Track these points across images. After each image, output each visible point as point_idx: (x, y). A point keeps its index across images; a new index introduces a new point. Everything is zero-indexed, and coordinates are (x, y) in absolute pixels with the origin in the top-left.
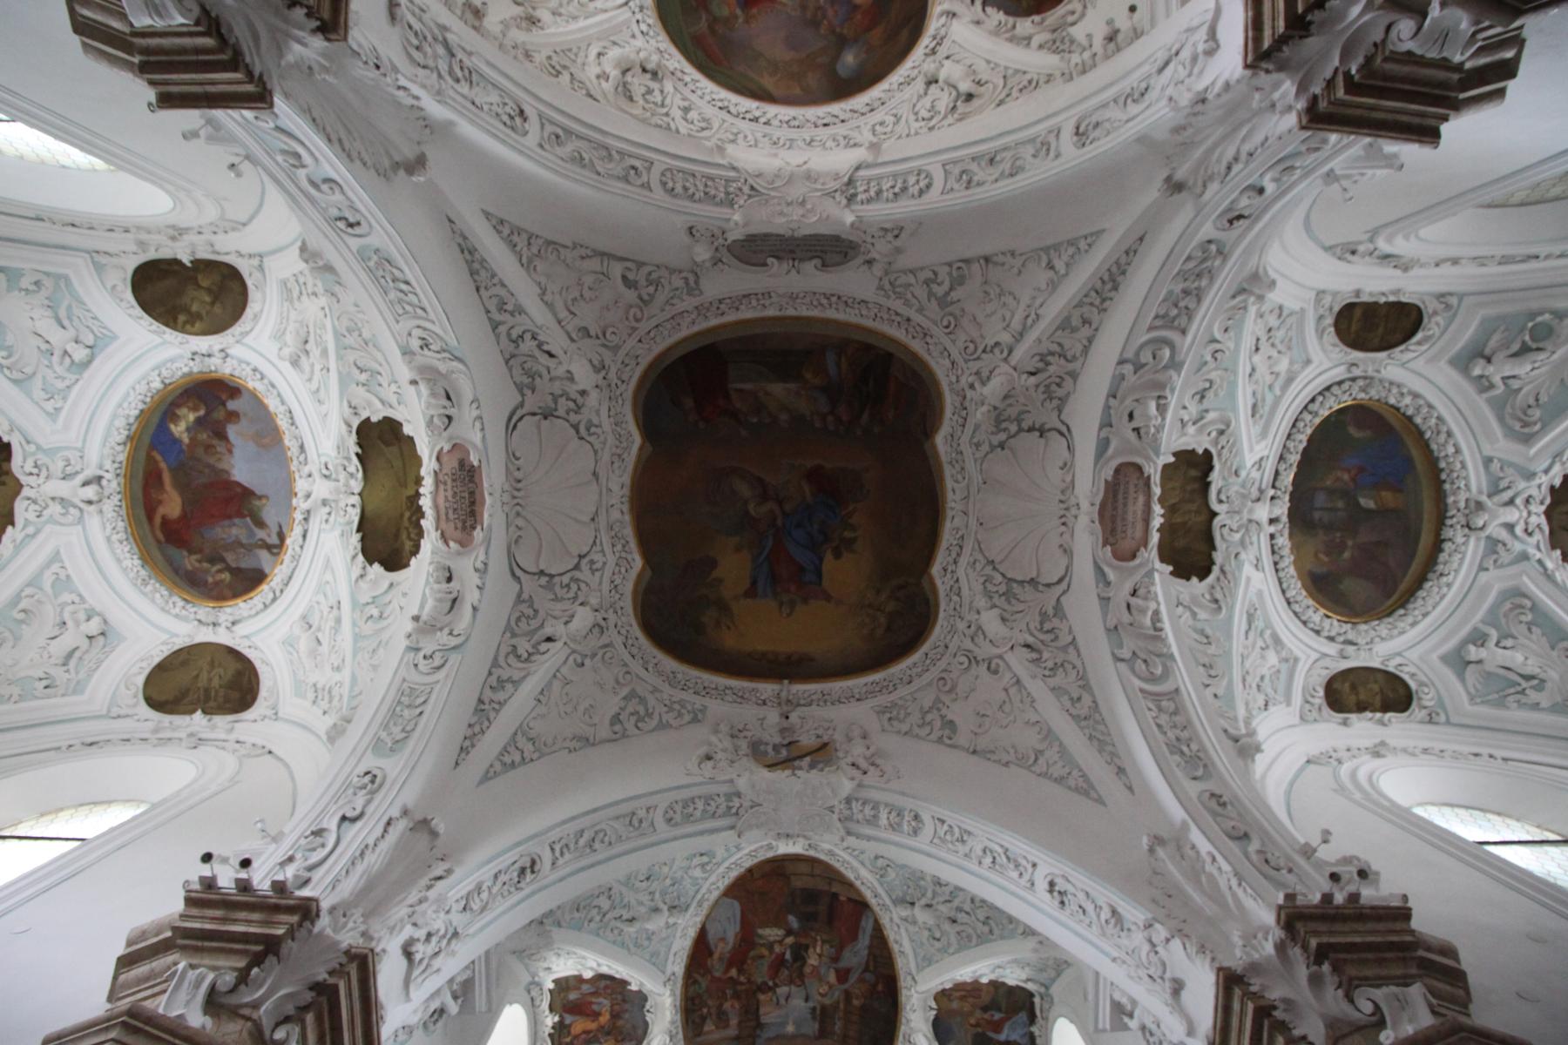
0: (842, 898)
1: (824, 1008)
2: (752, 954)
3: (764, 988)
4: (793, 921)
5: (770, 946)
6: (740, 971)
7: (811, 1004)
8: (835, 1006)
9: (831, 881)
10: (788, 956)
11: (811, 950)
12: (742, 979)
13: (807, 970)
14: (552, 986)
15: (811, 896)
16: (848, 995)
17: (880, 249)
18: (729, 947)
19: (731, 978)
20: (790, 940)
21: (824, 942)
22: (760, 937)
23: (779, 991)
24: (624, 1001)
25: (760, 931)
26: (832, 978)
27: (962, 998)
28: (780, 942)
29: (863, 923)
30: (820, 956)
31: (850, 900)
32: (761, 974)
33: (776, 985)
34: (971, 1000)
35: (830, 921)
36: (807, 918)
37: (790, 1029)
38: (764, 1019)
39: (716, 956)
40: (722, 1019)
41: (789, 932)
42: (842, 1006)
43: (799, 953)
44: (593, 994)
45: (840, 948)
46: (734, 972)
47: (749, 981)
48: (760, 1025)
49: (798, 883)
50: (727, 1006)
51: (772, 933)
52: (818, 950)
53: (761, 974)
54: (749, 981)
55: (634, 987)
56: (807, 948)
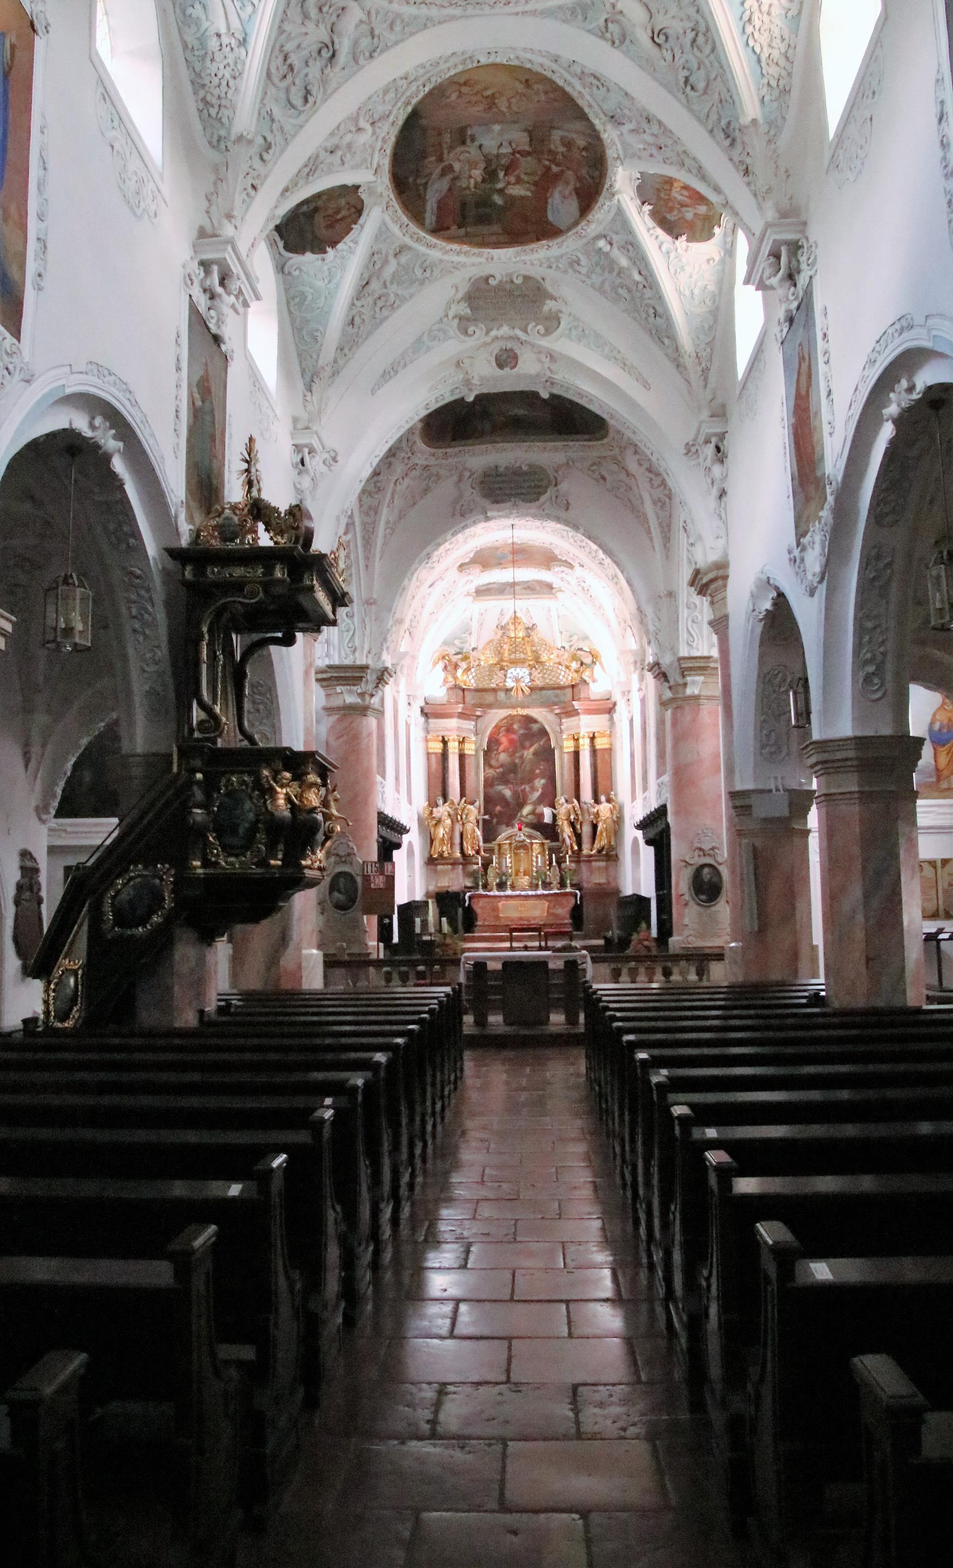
0: (454, 227)
1: (464, 143)
2: (537, 178)
3: (525, 154)
4: (498, 200)
5: (519, 181)
6: (548, 169)
7: (477, 143)
8: (451, 148)
9: (467, 235)
10: (501, 174)
11: (479, 179)
12: (547, 163)
13: (483, 165)
14: (717, 230)
15: (482, 220)
16: (440, 159)
17: (471, 494)
18: (559, 188)
19: (557, 165)
20: (500, 185)
21: (468, 188)
22: (528, 189)
23: (510, 150)
24: (658, 190)
25: (529, 194)
26: (457, 166)
27: (338, 211)
28: (509, 183)
29: (434, 218)
30: (471, 177)
31: (448, 228)
32: (527, 164)
33: (513, 154)
34: (330, 212)
35: (463, 205)
36: (484, 202)
37: (497, 128)
38: (526, 134)
39: (571, 187)
40: (568, 144)
41: (501, 191)
42: (445, 152)
43: (490, 175)
44: (682, 206)
45: (450, 190)
46: (555, 169)
47: (540, 160)
48: (530, 133)
49: (496, 228)
50: (561, 149)
51: (517, 191)
52: (472, 181)
53: (527, 164)
54: (540, 160)
55: (647, 208)
56: (484, 181)
